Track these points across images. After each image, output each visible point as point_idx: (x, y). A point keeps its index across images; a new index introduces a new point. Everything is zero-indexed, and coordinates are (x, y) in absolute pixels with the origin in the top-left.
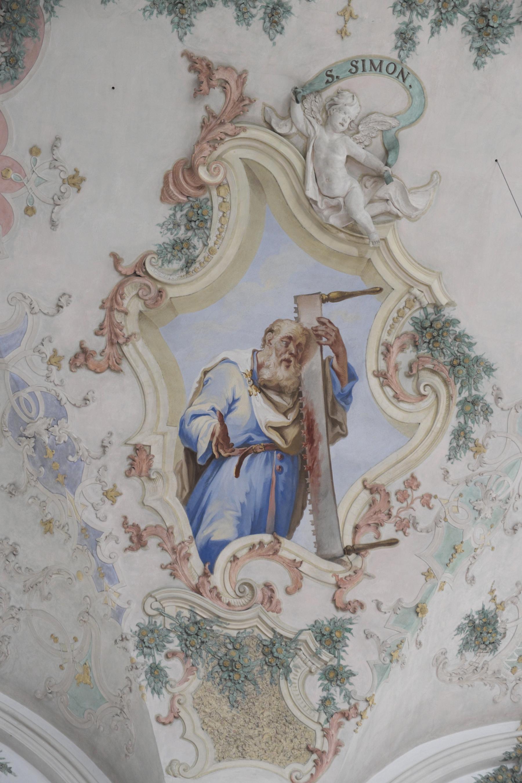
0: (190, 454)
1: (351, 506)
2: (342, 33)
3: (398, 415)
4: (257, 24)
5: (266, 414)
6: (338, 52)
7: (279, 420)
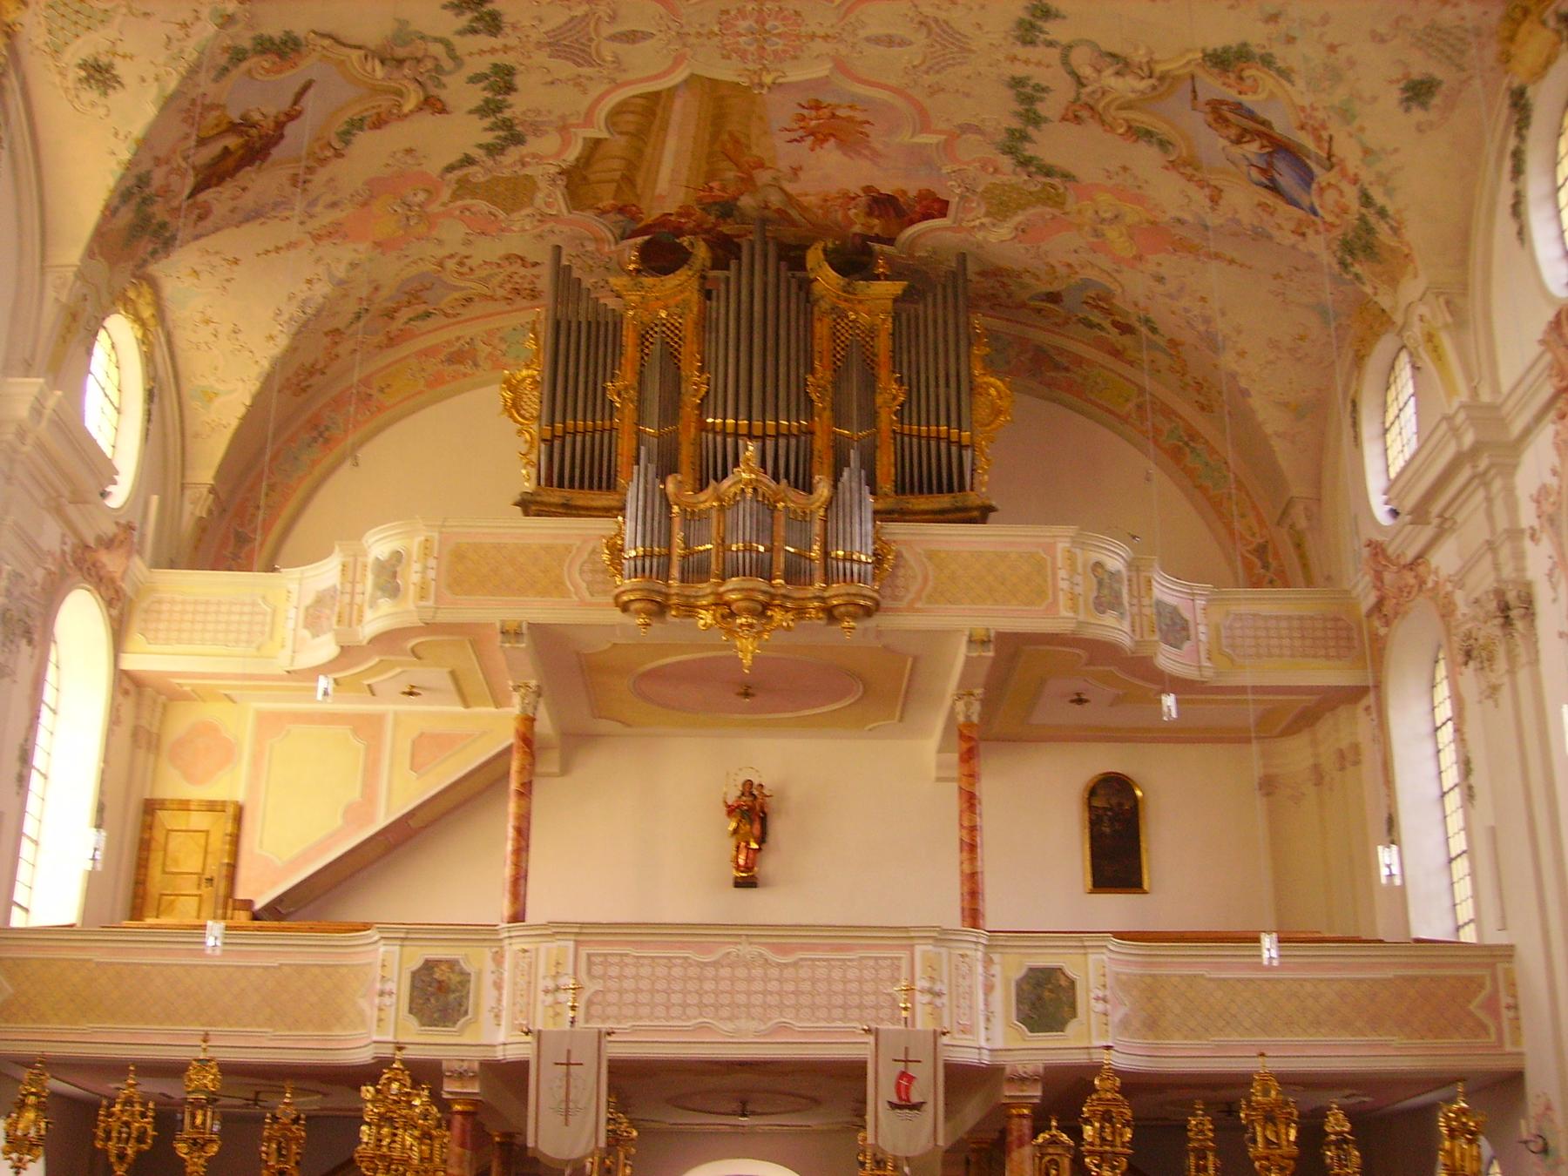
5: (1253, 148)
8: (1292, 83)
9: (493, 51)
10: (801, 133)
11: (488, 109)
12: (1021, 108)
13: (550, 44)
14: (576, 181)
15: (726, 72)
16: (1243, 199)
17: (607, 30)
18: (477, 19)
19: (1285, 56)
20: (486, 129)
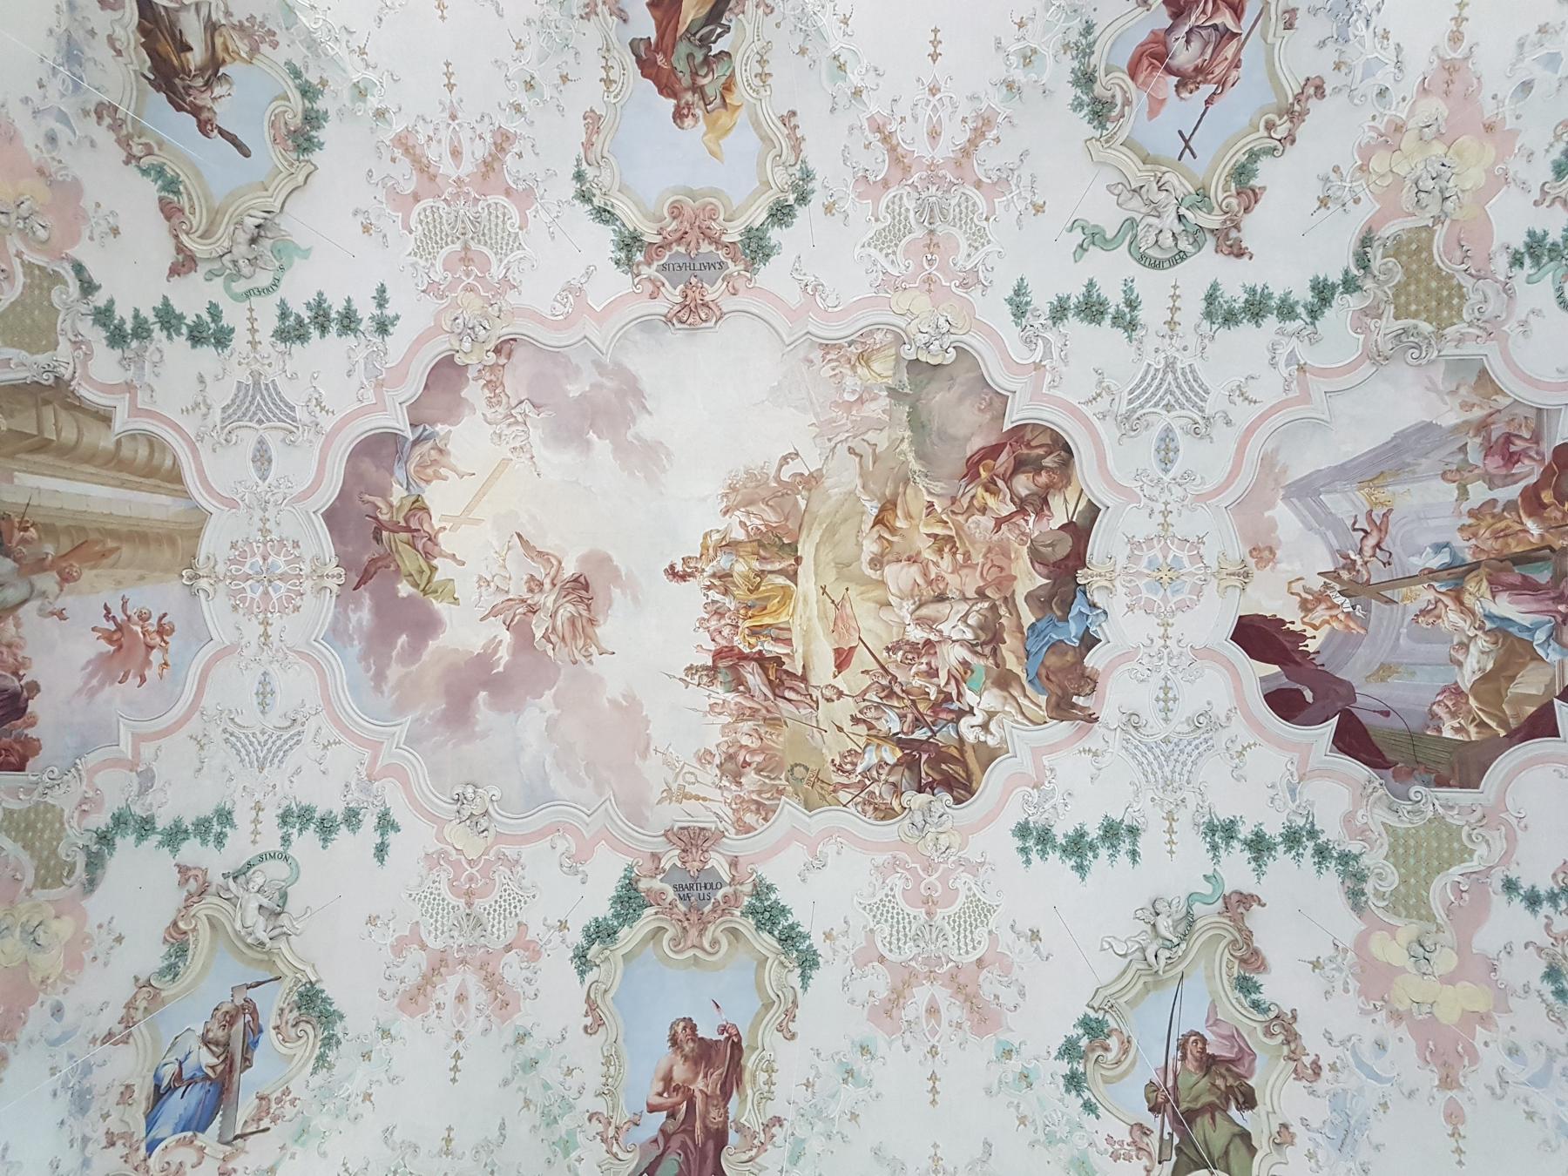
0: (157, 1087)
1: (246, 1107)
2: (254, 842)
3: (283, 1050)
4: (211, 844)
5: (207, 1058)
6: (251, 853)
7: (214, 1061)
8: (315, 1071)
9: (253, 331)
10: (120, 617)
11: (168, 318)
12: (188, 823)
13: (257, 383)
14: (55, 393)
15: (212, 544)
16: (131, 1066)
17: (274, 441)
18: (300, 321)
19: (341, 1058)
20: (136, 310)
